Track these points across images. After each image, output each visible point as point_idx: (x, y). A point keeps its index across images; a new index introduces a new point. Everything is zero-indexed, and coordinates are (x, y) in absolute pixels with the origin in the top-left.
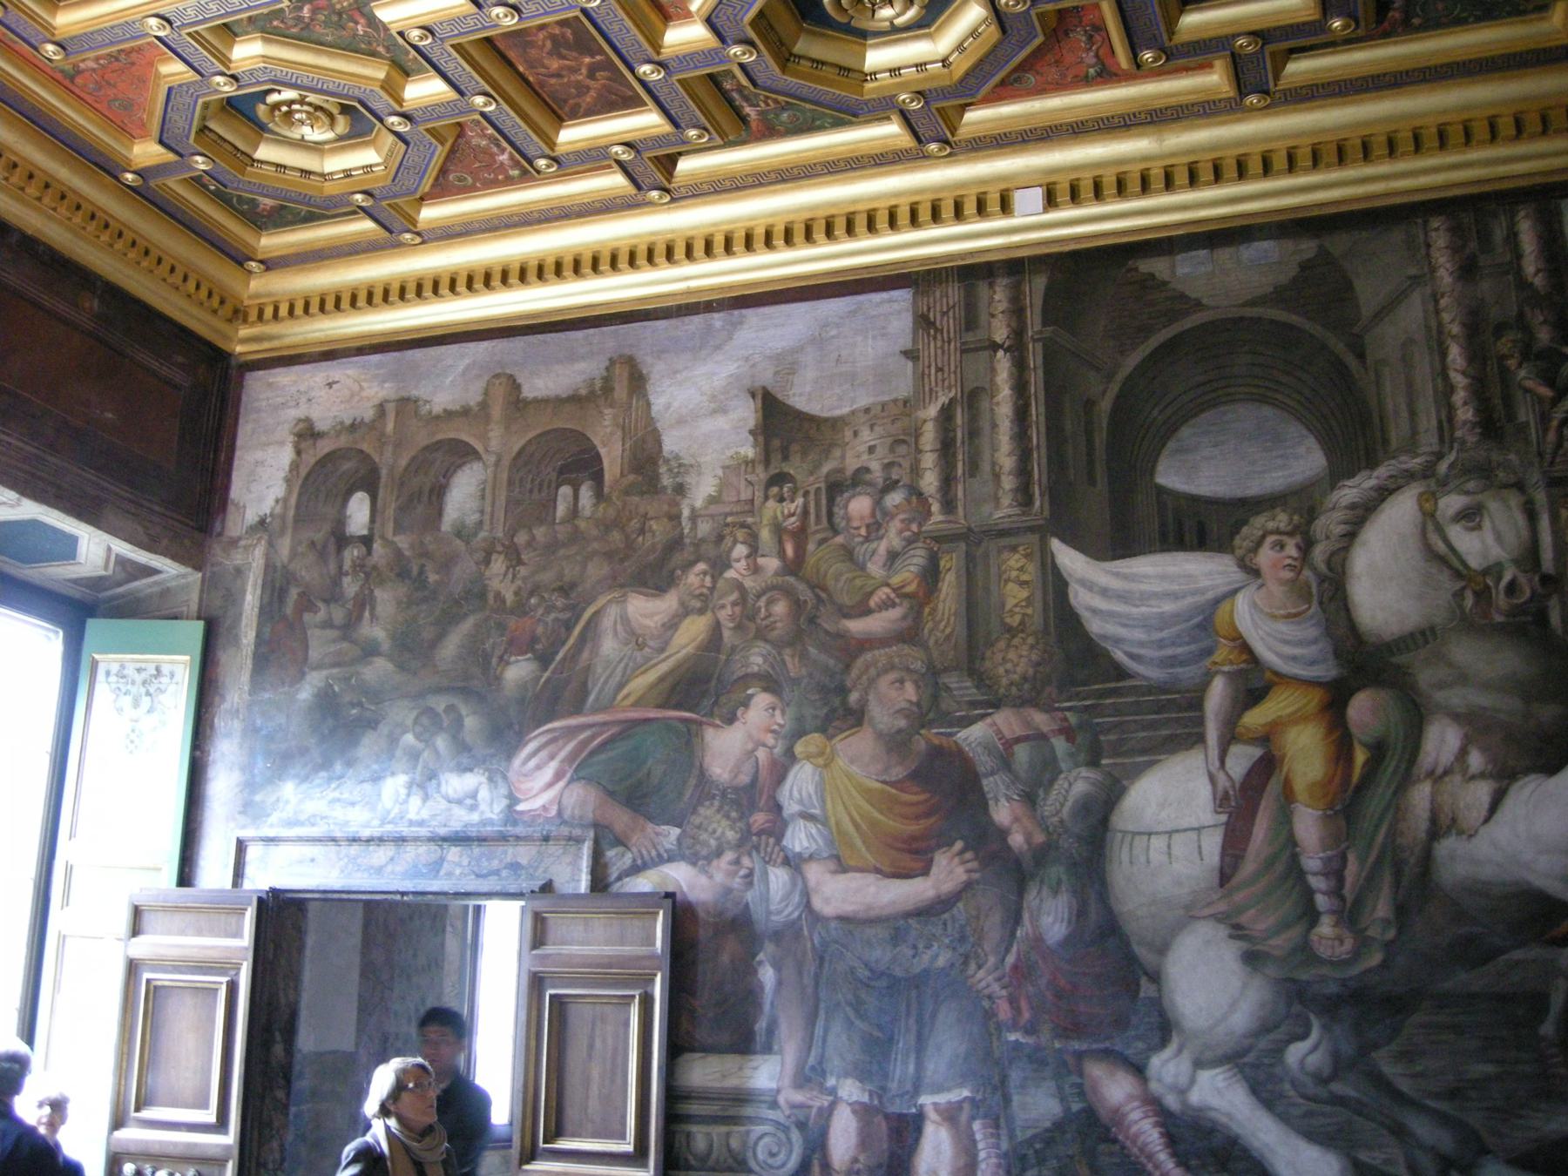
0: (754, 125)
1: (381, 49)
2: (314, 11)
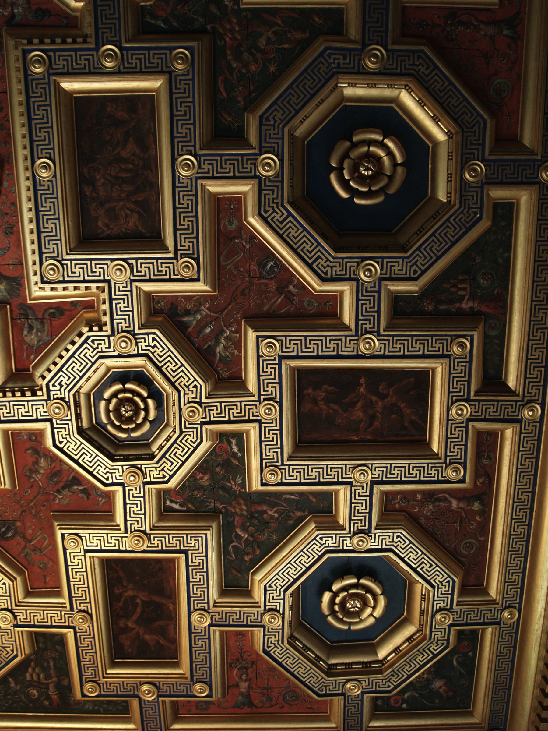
0: (484, 309)
1: (299, 514)
2: (245, 530)
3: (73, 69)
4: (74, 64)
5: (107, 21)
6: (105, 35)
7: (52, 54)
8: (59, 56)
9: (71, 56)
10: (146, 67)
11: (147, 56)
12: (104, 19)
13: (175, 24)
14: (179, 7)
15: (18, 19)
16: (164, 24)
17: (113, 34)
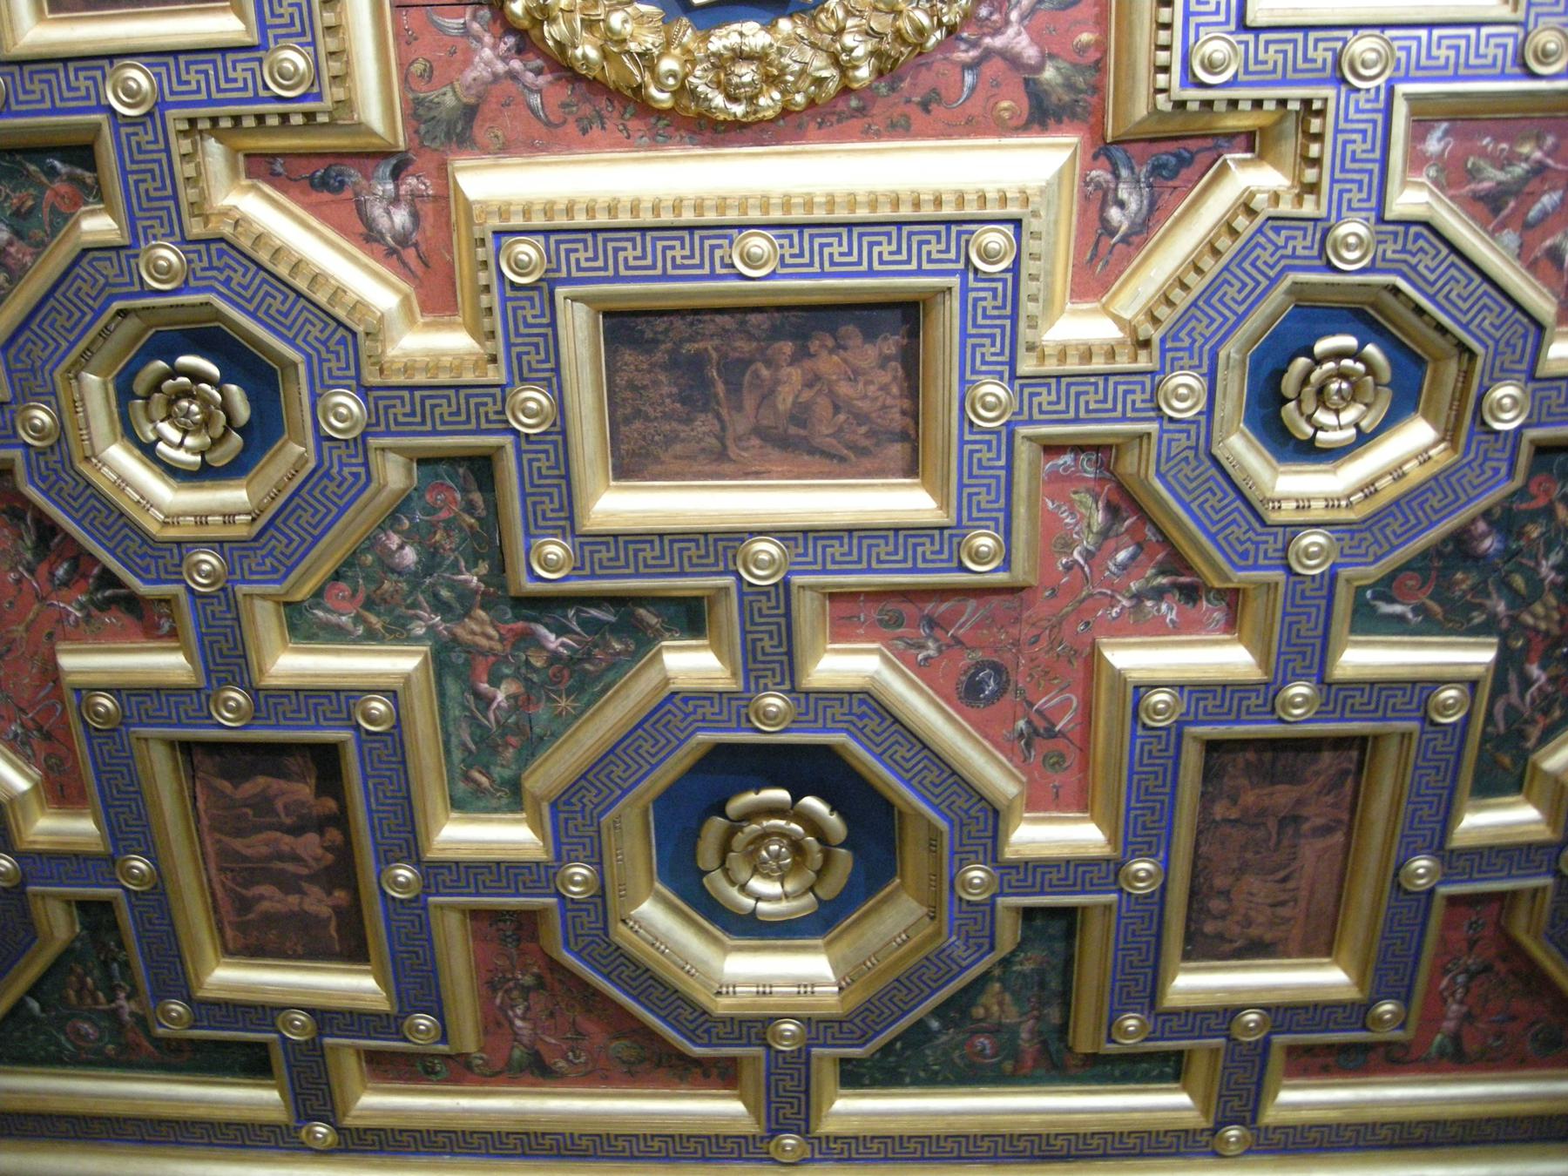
3: (214, 62)
4: (211, 72)
5: (149, 166)
6: (150, 137)
7: (262, 93)
8: (245, 88)
9: (219, 90)
10: (56, 72)
11: (57, 96)
12: (157, 172)
13: (32, 168)
14: (30, 203)
15: (385, 169)
16: (53, 168)
17: (134, 139)
